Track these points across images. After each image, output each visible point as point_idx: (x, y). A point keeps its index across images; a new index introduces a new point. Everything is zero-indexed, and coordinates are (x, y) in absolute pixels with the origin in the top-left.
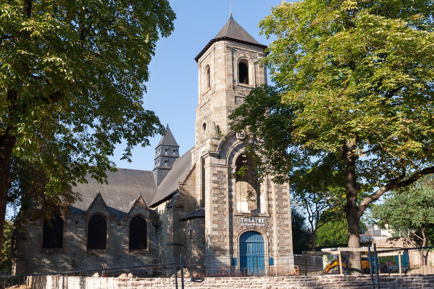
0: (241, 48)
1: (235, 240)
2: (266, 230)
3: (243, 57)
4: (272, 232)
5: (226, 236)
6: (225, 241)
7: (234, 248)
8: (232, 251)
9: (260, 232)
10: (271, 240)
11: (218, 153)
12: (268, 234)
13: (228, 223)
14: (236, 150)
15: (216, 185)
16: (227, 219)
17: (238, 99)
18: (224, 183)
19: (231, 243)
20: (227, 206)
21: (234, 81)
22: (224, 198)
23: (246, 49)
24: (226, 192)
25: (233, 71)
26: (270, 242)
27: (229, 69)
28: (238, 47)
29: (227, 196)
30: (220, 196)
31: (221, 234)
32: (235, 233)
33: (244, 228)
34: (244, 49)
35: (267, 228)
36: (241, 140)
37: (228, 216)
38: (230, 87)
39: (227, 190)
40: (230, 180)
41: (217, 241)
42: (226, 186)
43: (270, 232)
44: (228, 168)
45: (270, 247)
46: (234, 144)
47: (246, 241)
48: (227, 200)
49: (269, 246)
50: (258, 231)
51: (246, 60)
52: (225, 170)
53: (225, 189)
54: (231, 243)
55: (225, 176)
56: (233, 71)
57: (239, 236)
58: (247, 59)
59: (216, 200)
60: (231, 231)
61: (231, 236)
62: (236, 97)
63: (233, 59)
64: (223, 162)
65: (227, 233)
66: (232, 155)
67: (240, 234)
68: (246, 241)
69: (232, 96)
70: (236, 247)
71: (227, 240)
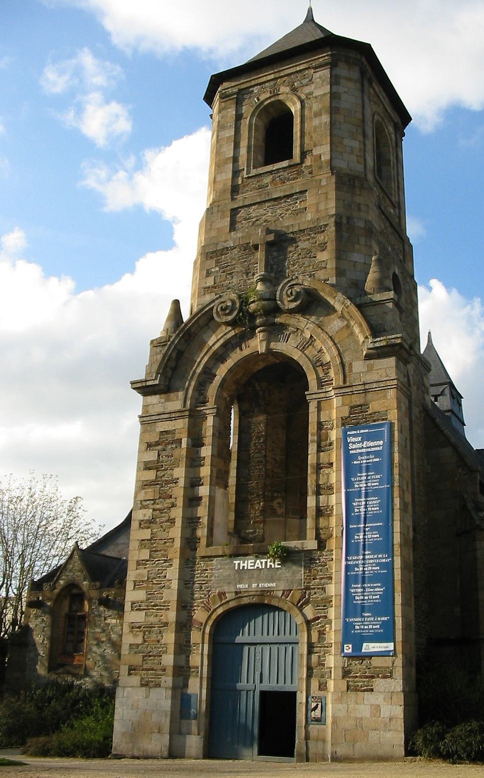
0: (264, 79)
1: (195, 636)
2: (303, 596)
3: (270, 98)
4: (327, 602)
5: (166, 624)
6: (163, 641)
7: (192, 663)
8: (182, 672)
9: (281, 605)
10: (321, 633)
11: (157, 382)
12: (309, 612)
13: (175, 585)
14: (219, 357)
15: (151, 475)
16: (173, 573)
17: (242, 213)
18: (176, 464)
19: (183, 648)
20: (176, 532)
21: (236, 173)
22: (169, 508)
23: (277, 75)
24: (178, 492)
25: (237, 146)
26: (315, 638)
27: (224, 149)
28: (253, 83)
29: (180, 502)
30: (158, 506)
31: (152, 619)
32: (199, 615)
33: (229, 596)
34: (272, 76)
35: (308, 588)
36: (227, 324)
37: (176, 563)
38: (224, 191)
39: (182, 483)
40: (198, 452)
41: (139, 640)
42: (180, 472)
43: (317, 604)
44: (190, 416)
45: (314, 658)
46: (210, 343)
47: (239, 639)
48: (178, 513)
49: (310, 652)
50: (274, 603)
51: (279, 101)
52: (181, 425)
53: (175, 481)
54: (183, 648)
55: (179, 441)
56: (237, 146)
57: (210, 623)
58: (281, 97)
59: (147, 518)
60: (185, 605)
61: (184, 626)
62: (234, 212)
63: (239, 117)
64: (176, 403)
65: (171, 616)
66: (208, 374)
67: (214, 617)
68: (239, 639)
69: (223, 212)
70: (200, 657)
71: (170, 638)
